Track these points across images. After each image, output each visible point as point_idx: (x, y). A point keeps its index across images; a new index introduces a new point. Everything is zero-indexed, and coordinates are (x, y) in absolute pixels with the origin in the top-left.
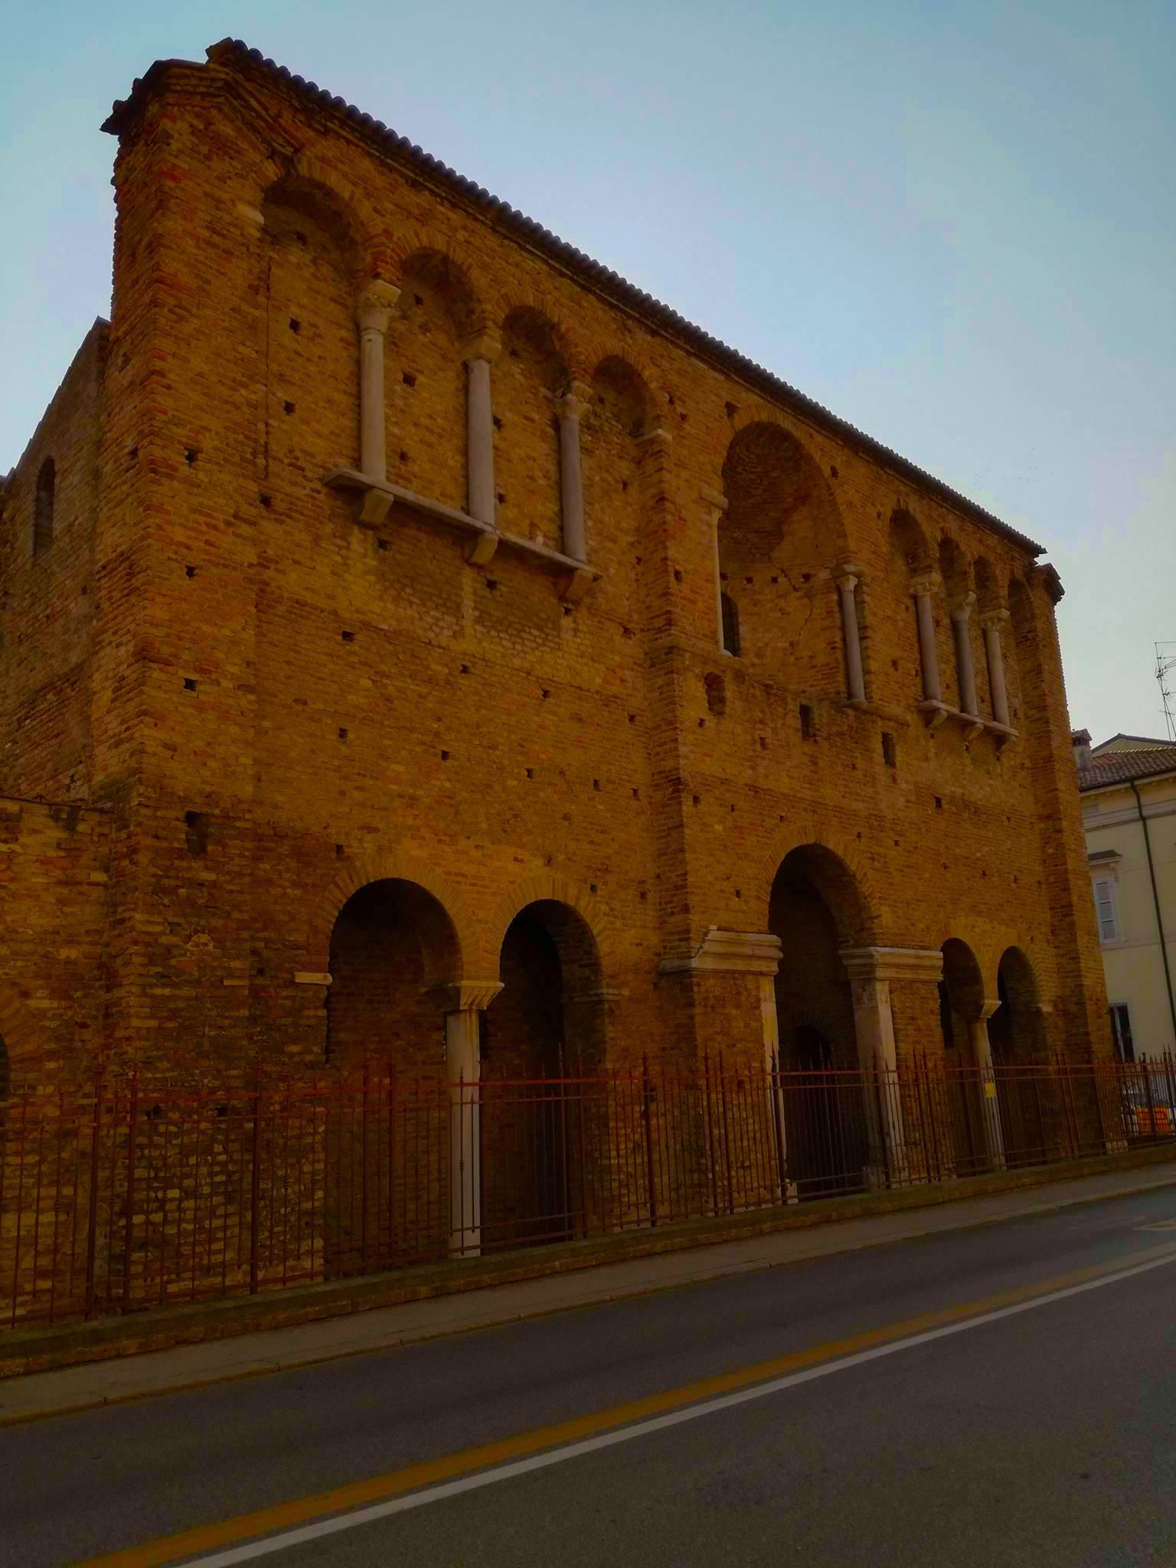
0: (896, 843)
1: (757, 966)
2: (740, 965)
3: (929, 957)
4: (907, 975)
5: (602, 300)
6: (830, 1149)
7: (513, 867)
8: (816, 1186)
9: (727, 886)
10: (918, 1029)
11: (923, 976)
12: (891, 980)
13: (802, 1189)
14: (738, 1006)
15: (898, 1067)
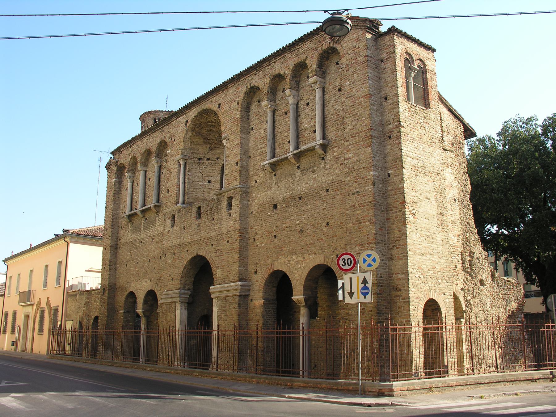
0: (228, 242)
1: (174, 300)
2: (170, 300)
3: (231, 286)
4: (224, 294)
5: (157, 131)
6: (198, 353)
7: (145, 284)
8: (192, 364)
9: (170, 278)
10: (226, 315)
11: (230, 293)
12: (218, 297)
13: (190, 364)
14: (169, 312)
15: (218, 329)
